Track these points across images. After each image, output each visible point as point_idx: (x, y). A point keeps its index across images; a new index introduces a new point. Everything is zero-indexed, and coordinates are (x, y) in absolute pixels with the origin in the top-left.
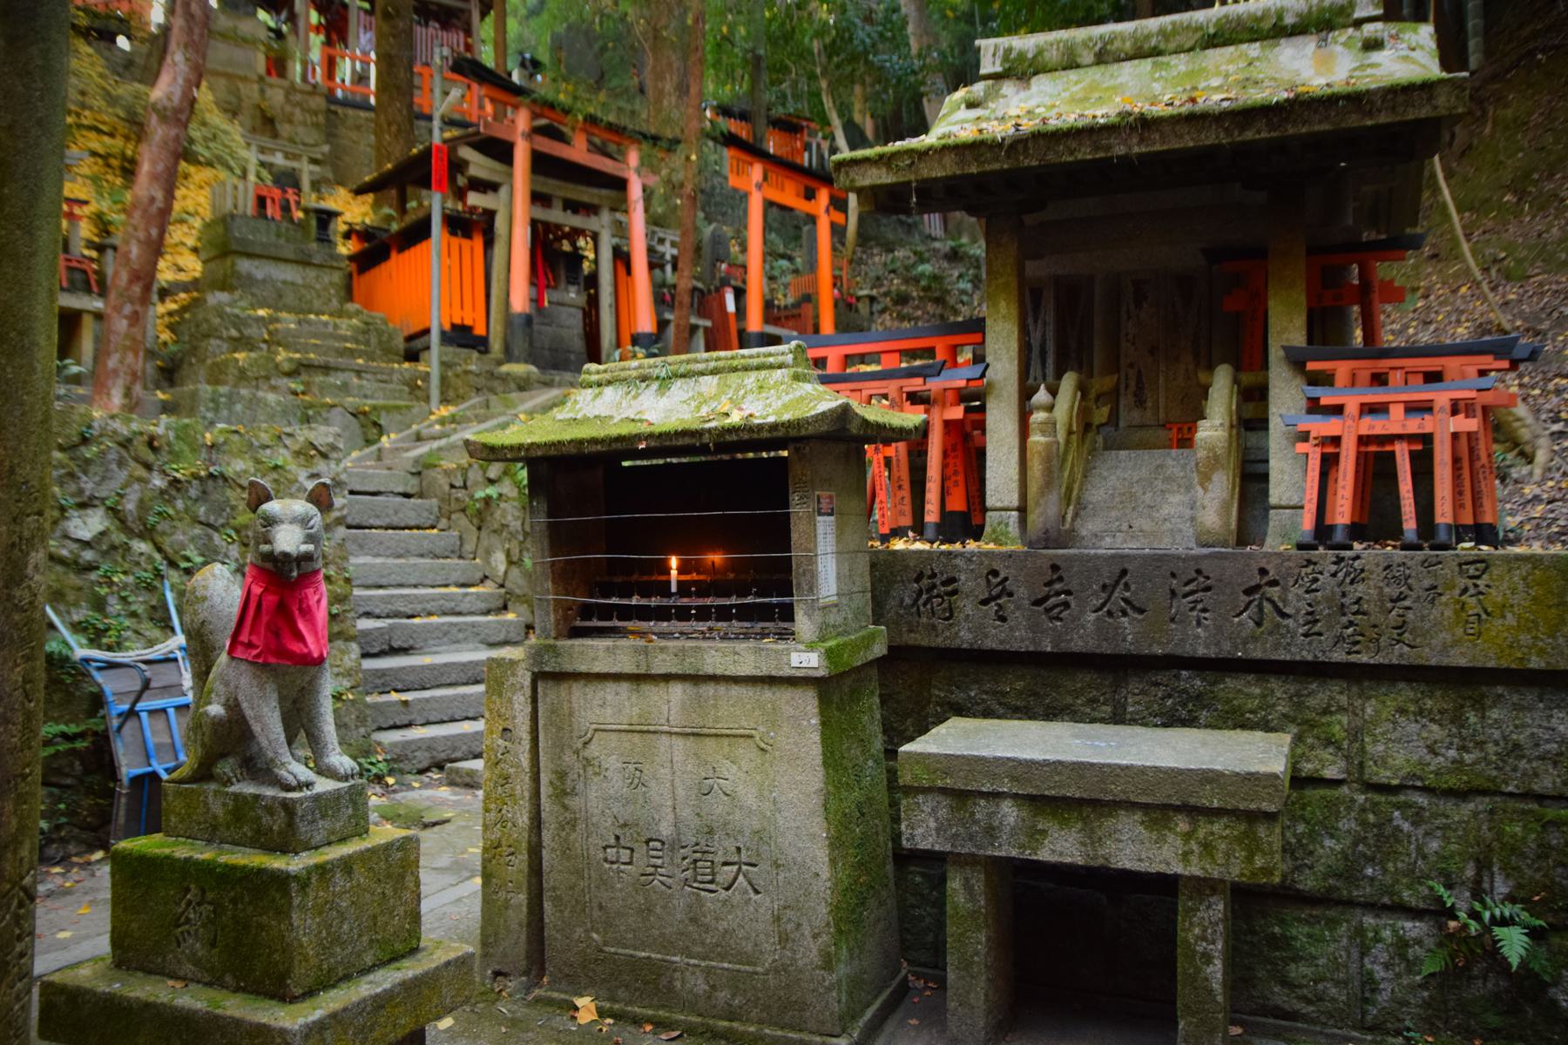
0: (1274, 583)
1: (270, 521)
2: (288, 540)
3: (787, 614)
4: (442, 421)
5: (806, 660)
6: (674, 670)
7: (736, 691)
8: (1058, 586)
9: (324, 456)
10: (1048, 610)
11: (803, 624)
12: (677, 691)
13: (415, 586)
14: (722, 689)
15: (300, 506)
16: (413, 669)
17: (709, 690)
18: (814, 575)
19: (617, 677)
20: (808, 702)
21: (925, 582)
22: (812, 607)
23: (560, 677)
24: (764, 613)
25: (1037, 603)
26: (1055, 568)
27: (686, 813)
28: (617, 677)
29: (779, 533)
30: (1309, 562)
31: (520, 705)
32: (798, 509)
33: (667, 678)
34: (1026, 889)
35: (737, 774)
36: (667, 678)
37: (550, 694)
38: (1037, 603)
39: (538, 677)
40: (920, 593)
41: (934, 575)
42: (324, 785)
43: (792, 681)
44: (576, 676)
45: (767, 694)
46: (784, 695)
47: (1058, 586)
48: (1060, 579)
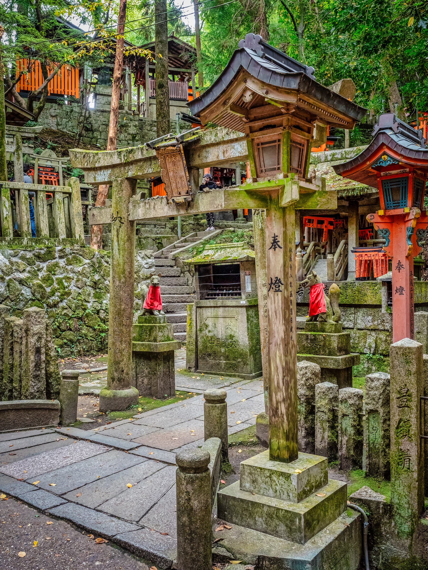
1: (153, 279)
2: (156, 281)
3: (240, 294)
4: (182, 242)
5: (243, 302)
7: (232, 309)
9: (149, 258)
11: (243, 296)
12: (221, 309)
13: (174, 294)
14: (229, 308)
15: (157, 277)
16: (174, 317)
17: (227, 309)
18: (245, 287)
19: (211, 307)
22: (245, 292)
23: (200, 307)
25: (297, 293)
27: (223, 332)
28: (211, 307)
29: (238, 279)
31: (194, 312)
32: (242, 274)
33: (220, 307)
35: (232, 323)
36: (220, 307)
37: (199, 310)
38: (297, 293)
39: (197, 307)
42: (160, 315)
44: (204, 307)
45: (237, 309)
46: (240, 309)
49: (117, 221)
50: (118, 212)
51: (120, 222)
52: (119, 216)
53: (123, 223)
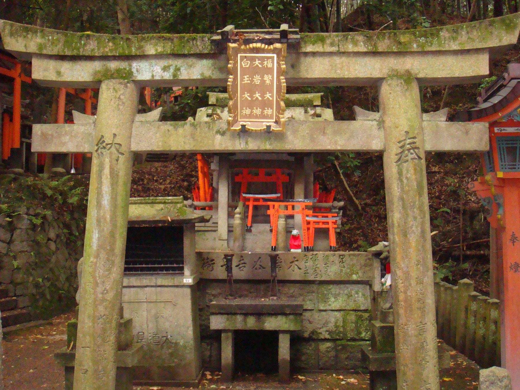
0: (297, 260)
3: (182, 269)
6: (149, 284)
8: (242, 262)
10: (240, 268)
20: (188, 291)
21: (206, 261)
24: (174, 269)
26: (242, 257)
30: (306, 255)
34: (241, 338)
40: (204, 264)
41: (208, 259)
43: (183, 286)
47: (242, 262)
48: (243, 260)
49: (113, 150)
50: (115, 135)
51: (118, 151)
52: (117, 140)
53: (122, 154)
